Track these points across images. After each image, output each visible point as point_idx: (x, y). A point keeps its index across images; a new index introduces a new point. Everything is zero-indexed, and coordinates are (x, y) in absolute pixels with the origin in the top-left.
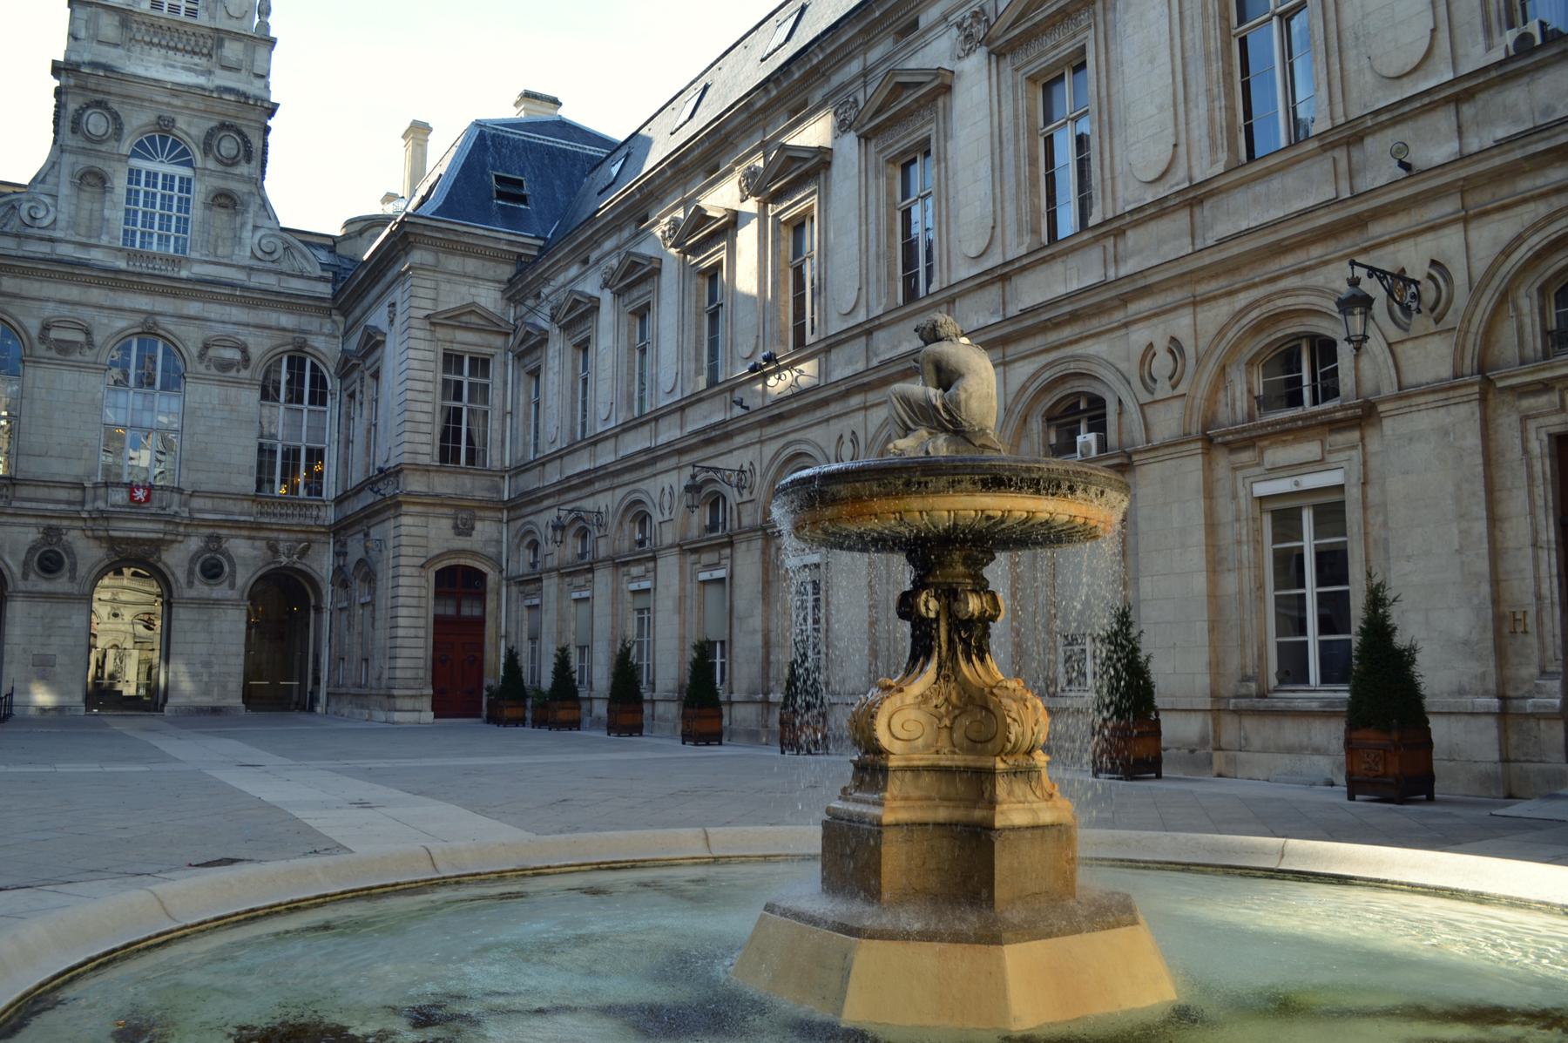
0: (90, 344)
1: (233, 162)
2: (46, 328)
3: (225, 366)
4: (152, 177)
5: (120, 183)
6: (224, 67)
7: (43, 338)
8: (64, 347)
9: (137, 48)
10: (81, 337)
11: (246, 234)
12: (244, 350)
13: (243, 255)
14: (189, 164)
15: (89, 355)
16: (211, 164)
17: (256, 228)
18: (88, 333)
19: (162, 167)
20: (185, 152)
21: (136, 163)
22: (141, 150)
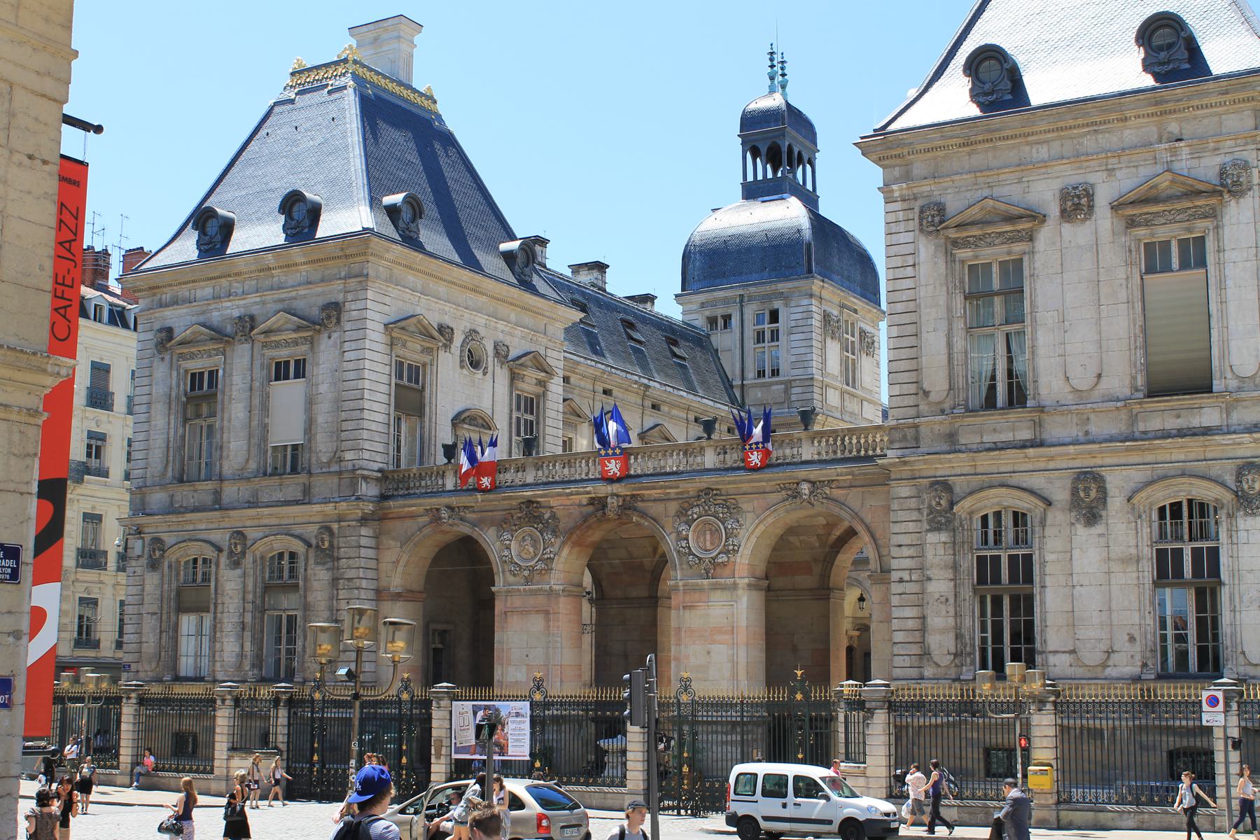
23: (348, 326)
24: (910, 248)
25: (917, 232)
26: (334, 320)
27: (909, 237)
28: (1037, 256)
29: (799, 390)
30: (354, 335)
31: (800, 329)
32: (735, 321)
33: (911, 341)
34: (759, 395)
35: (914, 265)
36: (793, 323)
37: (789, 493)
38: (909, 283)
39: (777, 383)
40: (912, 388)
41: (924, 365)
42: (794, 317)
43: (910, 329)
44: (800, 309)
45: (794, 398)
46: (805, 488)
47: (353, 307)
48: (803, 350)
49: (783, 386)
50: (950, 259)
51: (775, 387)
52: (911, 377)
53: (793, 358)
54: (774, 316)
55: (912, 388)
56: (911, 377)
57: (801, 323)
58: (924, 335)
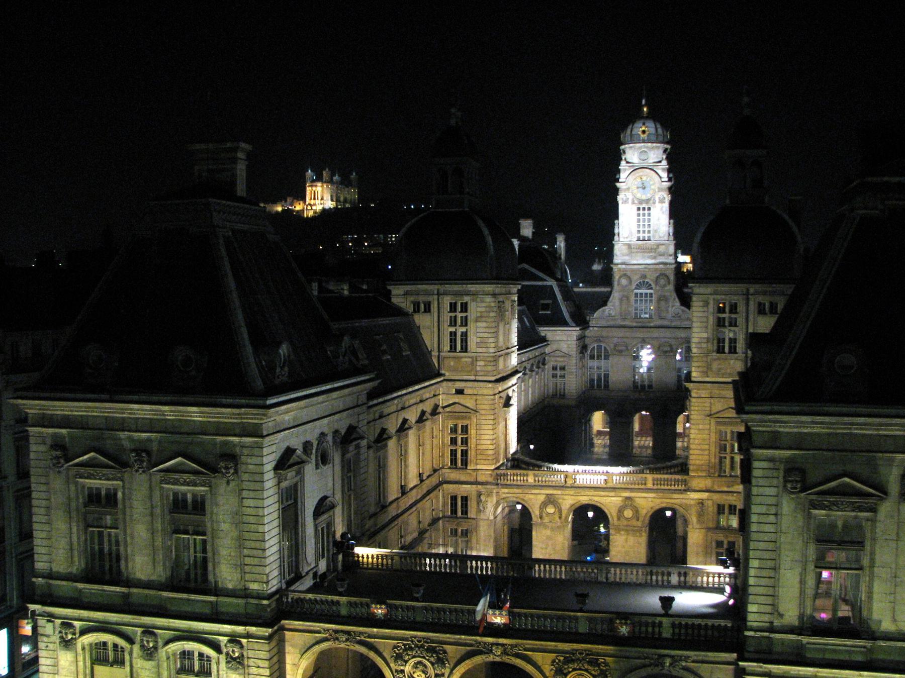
0: (628, 349)
1: (665, 286)
2: (616, 345)
3: (666, 352)
4: (641, 294)
5: (633, 298)
6: (660, 255)
7: (615, 349)
8: (620, 351)
9: (633, 255)
10: (624, 348)
11: (670, 309)
12: (670, 346)
13: (669, 316)
14: (651, 289)
15: (626, 353)
16: (658, 288)
17: (673, 306)
18: (627, 347)
19: (643, 291)
20: (650, 285)
21: (636, 291)
22: (639, 286)
23: (245, 477)
24: (773, 501)
25: (781, 489)
26: (232, 471)
27: (773, 491)
28: (878, 524)
29: (482, 363)
30: (252, 486)
31: (484, 319)
32: (435, 307)
33: (771, 573)
34: (452, 363)
35: (776, 515)
36: (479, 315)
37: (652, 661)
38: (771, 528)
39: (466, 357)
40: (768, 609)
41: (780, 593)
42: (479, 309)
43: (770, 564)
44: (484, 305)
45: (478, 368)
46: (668, 662)
47: (249, 461)
48: (486, 335)
49: (470, 360)
50: (809, 516)
51: (464, 360)
52: (769, 600)
53: (478, 340)
54: (464, 308)
55: (768, 609)
56: (769, 600)
57: (485, 314)
58: (782, 571)
